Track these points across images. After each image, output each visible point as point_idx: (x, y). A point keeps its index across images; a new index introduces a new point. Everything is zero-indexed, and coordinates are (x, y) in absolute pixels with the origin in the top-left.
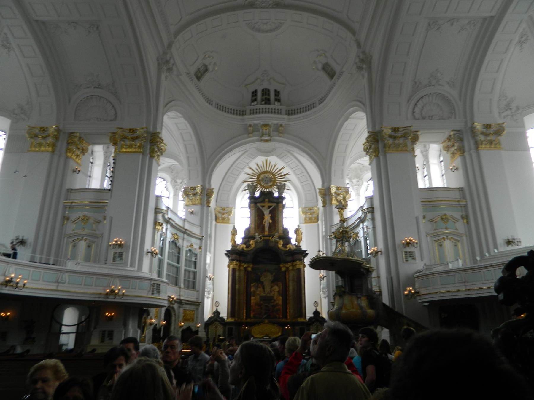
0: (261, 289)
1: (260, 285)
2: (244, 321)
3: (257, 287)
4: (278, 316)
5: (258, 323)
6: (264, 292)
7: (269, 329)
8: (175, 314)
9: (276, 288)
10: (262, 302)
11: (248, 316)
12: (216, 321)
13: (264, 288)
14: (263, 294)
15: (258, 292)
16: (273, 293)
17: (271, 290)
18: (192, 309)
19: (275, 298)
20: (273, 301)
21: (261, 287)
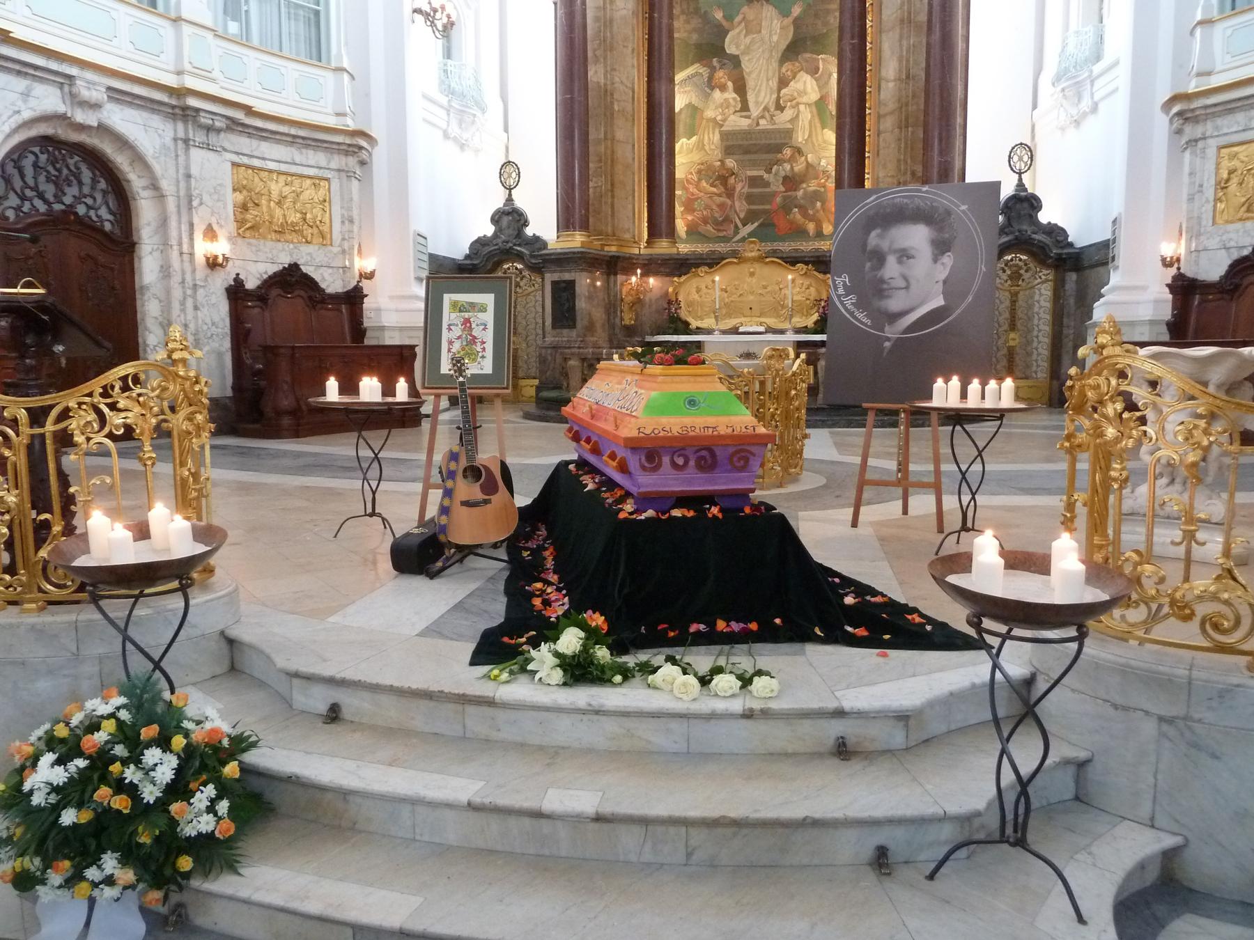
0: (731, 95)
1: (720, 75)
2: (641, 249)
3: (711, 84)
4: (811, 227)
5: (712, 262)
6: (745, 107)
7: (765, 287)
8: (155, 186)
9: (806, 87)
10: (731, 163)
11: (660, 225)
12: (507, 254)
13: (741, 89)
14: (738, 122)
15: (710, 113)
16: (788, 114)
17: (778, 98)
18: (311, 172)
19: (800, 138)
20: (787, 152)
21: (730, 84)
